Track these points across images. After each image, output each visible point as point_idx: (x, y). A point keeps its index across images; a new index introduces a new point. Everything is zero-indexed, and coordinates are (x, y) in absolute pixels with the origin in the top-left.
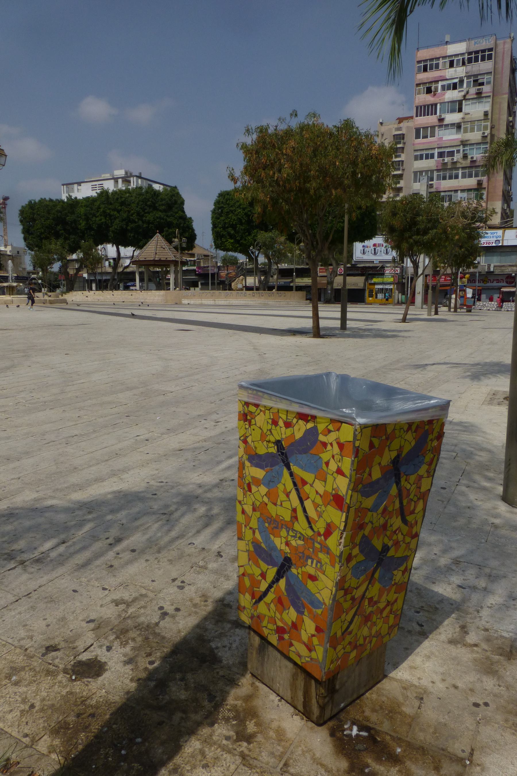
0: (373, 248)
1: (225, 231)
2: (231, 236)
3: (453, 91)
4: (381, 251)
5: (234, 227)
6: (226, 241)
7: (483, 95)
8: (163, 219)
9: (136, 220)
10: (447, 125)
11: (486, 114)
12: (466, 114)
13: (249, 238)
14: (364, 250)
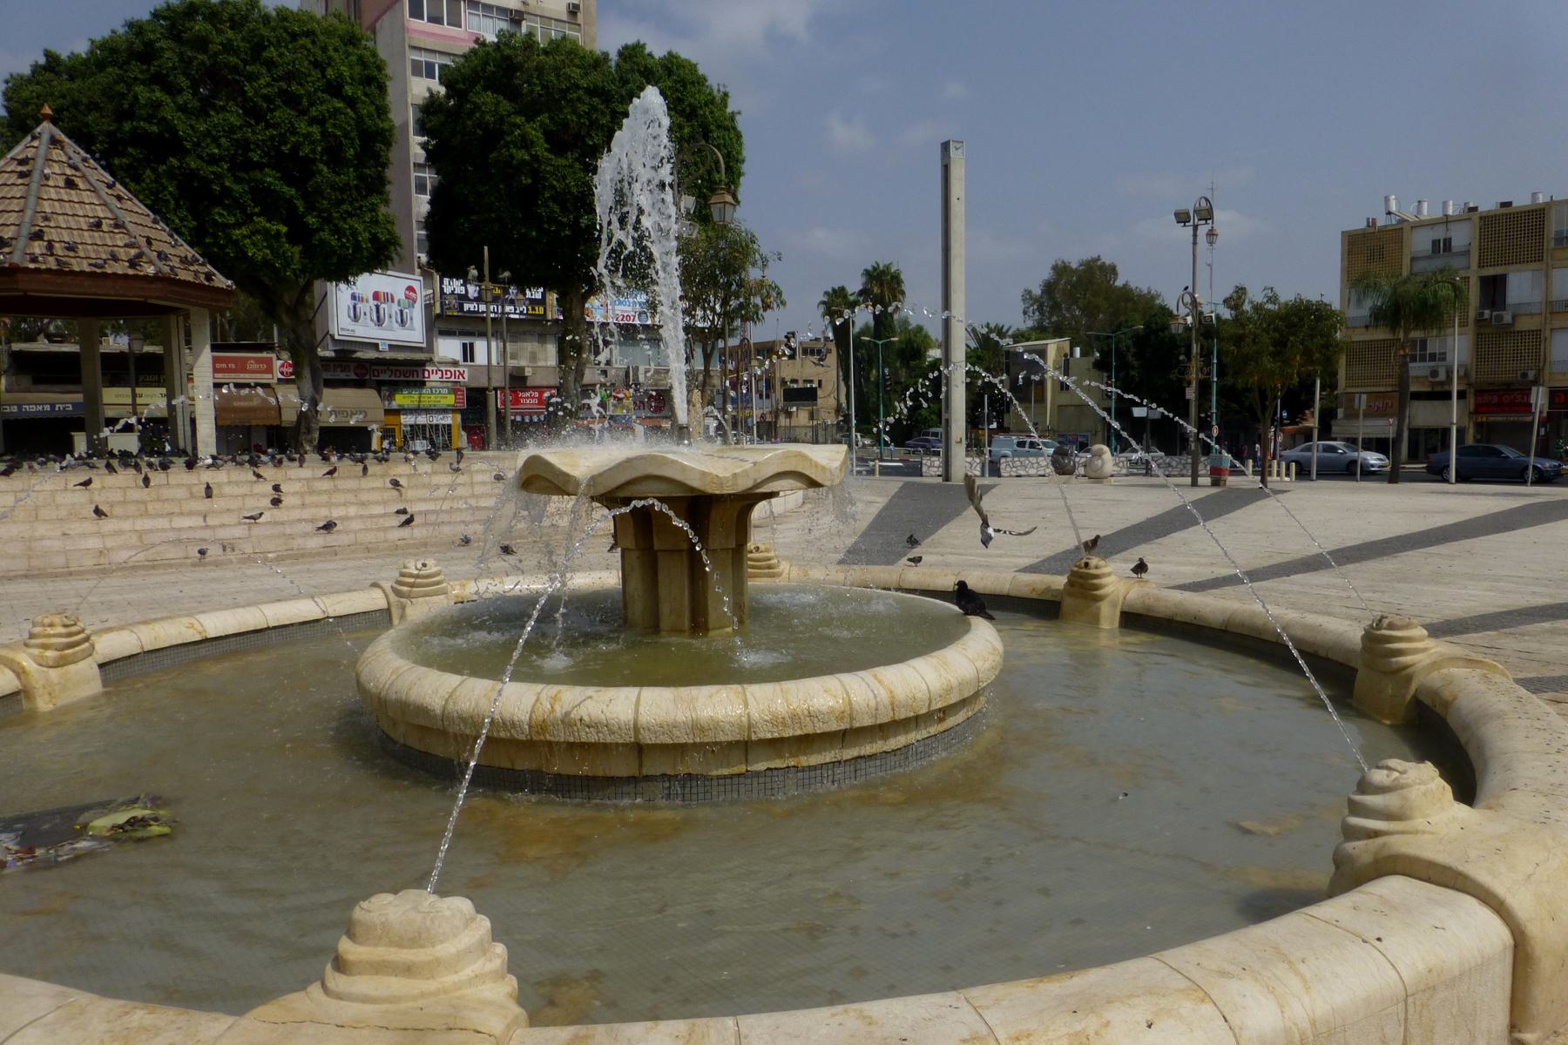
0: (372, 303)
1: (238, 181)
2: (269, 203)
4: (390, 317)
6: (238, 225)
13: (360, 228)
14: (355, 308)
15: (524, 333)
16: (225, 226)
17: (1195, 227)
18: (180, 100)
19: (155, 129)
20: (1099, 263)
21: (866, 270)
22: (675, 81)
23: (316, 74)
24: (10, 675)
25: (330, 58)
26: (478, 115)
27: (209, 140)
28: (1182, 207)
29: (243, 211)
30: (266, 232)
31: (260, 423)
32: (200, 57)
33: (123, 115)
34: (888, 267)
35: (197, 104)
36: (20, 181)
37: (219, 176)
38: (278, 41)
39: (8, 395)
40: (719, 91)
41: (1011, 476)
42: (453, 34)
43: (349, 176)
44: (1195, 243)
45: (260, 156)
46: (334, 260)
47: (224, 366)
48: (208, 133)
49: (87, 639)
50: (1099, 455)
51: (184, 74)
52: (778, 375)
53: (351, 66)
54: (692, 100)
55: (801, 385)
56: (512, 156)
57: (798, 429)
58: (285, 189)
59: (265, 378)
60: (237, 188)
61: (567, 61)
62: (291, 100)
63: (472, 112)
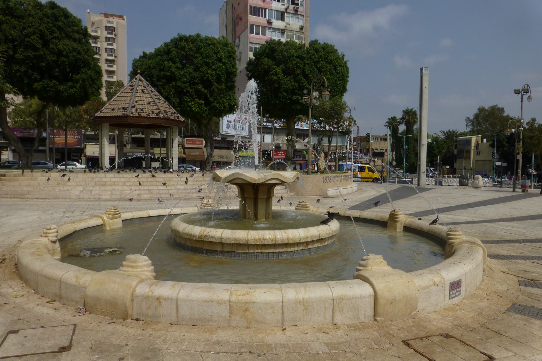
0: (233, 123)
1: (191, 88)
2: (199, 94)
3: (278, 3)
5: (208, 84)
6: (191, 101)
7: (299, 13)
8: (79, 53)
9: (39, 46)
10: (274, 29)
11: (301, 28)
12: (287, 24)
13: (225, 101)
15: (281, 133)
16: (187, 102)
17: (522, 96)
18: (176, 65)
19: (169, 74)
20: (497, 107)
21: (404, 111)
22: (325, 52)
23: (215, 56)
24: (101, 220)
25: (219, 51)
26: (263, 66)
27: (184, 77)
28: (517, 88)
29: (192, 97)
30: (198, 103)
31: (198, 160)
32: (182, 52)
33: (162, 70)
34: (412, 109)
35: (181, 66)
36: (131, 91)
37: (186, 87)
38: (204, 47)
39: (130, 150)
40: (341, 54)
41: (446, 185)
42: (263, 38)
43: (223, 86)
44: (522, 101)
45: (198, 81)
46: (218, 111)
47: (189, 142)
48: (183, 75)
49: (119, 213)
50: (478, 179)
51: (178, 57)
52: (371, 147)
53: (225, 53)
54: (331, 58)
55: (379, 151)
56: (272, 78)
57: (377, 167)
58: (204, 90)
59: (200, 146)
60: (191, 90)
61: (290, 48)
62: (207, 64)
63: (261, 65)
